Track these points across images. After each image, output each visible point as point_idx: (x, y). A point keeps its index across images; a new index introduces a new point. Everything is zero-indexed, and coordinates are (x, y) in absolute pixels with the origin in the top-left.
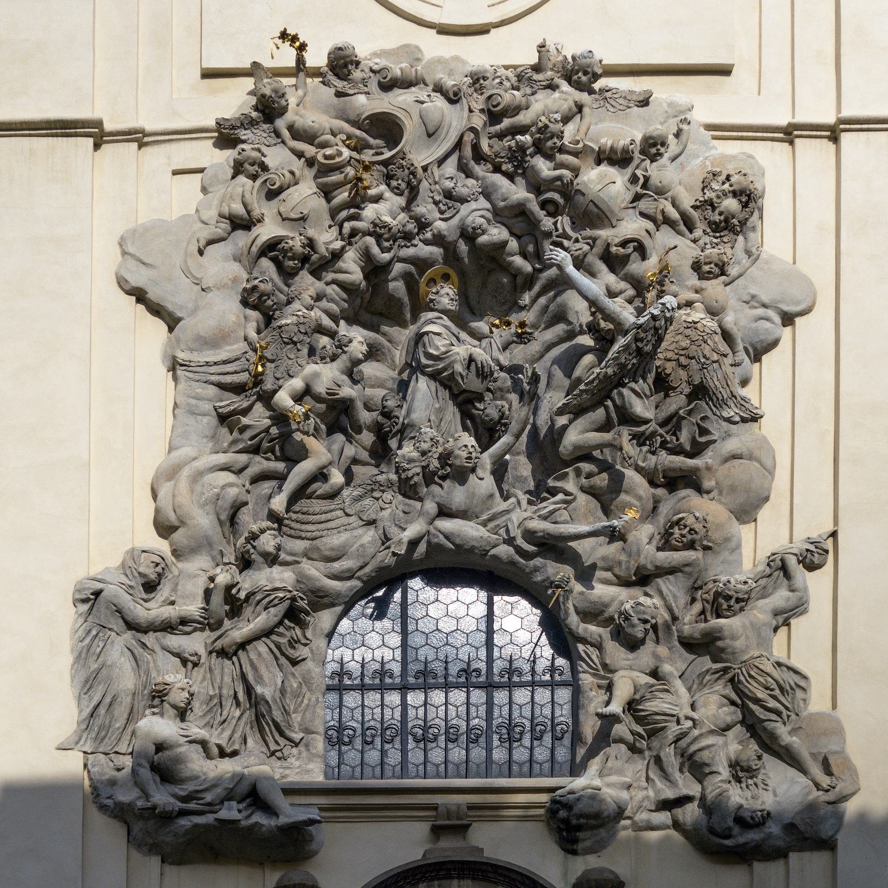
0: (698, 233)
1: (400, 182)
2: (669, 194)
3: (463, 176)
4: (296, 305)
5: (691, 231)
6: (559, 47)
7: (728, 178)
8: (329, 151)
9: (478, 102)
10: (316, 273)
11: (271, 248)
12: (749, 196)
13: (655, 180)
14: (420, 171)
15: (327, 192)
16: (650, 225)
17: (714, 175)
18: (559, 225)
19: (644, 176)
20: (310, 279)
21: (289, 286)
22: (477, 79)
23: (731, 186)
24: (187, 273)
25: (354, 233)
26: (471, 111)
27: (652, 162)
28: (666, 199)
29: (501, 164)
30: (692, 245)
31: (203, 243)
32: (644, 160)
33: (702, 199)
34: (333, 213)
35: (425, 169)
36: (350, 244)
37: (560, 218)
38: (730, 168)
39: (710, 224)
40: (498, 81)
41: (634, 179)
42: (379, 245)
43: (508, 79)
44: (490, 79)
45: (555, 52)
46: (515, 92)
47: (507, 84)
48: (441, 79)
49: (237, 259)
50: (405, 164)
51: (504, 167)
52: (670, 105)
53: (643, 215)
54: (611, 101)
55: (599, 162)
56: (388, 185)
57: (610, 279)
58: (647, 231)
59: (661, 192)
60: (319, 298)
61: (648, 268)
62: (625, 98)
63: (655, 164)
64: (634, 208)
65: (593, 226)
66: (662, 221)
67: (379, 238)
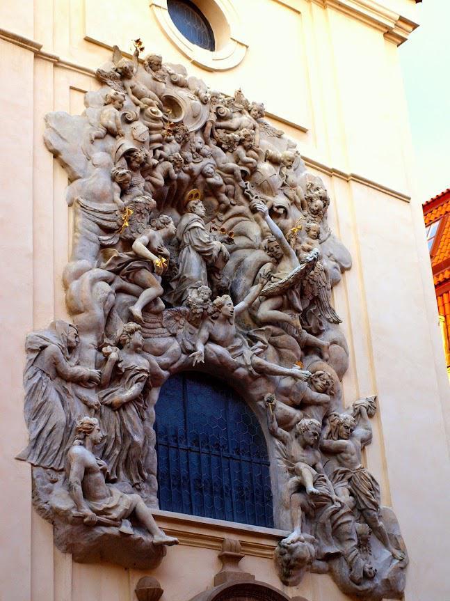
16: (289, 202)
26: (210, 111)
29: (222, 143)
51: (223, 146)
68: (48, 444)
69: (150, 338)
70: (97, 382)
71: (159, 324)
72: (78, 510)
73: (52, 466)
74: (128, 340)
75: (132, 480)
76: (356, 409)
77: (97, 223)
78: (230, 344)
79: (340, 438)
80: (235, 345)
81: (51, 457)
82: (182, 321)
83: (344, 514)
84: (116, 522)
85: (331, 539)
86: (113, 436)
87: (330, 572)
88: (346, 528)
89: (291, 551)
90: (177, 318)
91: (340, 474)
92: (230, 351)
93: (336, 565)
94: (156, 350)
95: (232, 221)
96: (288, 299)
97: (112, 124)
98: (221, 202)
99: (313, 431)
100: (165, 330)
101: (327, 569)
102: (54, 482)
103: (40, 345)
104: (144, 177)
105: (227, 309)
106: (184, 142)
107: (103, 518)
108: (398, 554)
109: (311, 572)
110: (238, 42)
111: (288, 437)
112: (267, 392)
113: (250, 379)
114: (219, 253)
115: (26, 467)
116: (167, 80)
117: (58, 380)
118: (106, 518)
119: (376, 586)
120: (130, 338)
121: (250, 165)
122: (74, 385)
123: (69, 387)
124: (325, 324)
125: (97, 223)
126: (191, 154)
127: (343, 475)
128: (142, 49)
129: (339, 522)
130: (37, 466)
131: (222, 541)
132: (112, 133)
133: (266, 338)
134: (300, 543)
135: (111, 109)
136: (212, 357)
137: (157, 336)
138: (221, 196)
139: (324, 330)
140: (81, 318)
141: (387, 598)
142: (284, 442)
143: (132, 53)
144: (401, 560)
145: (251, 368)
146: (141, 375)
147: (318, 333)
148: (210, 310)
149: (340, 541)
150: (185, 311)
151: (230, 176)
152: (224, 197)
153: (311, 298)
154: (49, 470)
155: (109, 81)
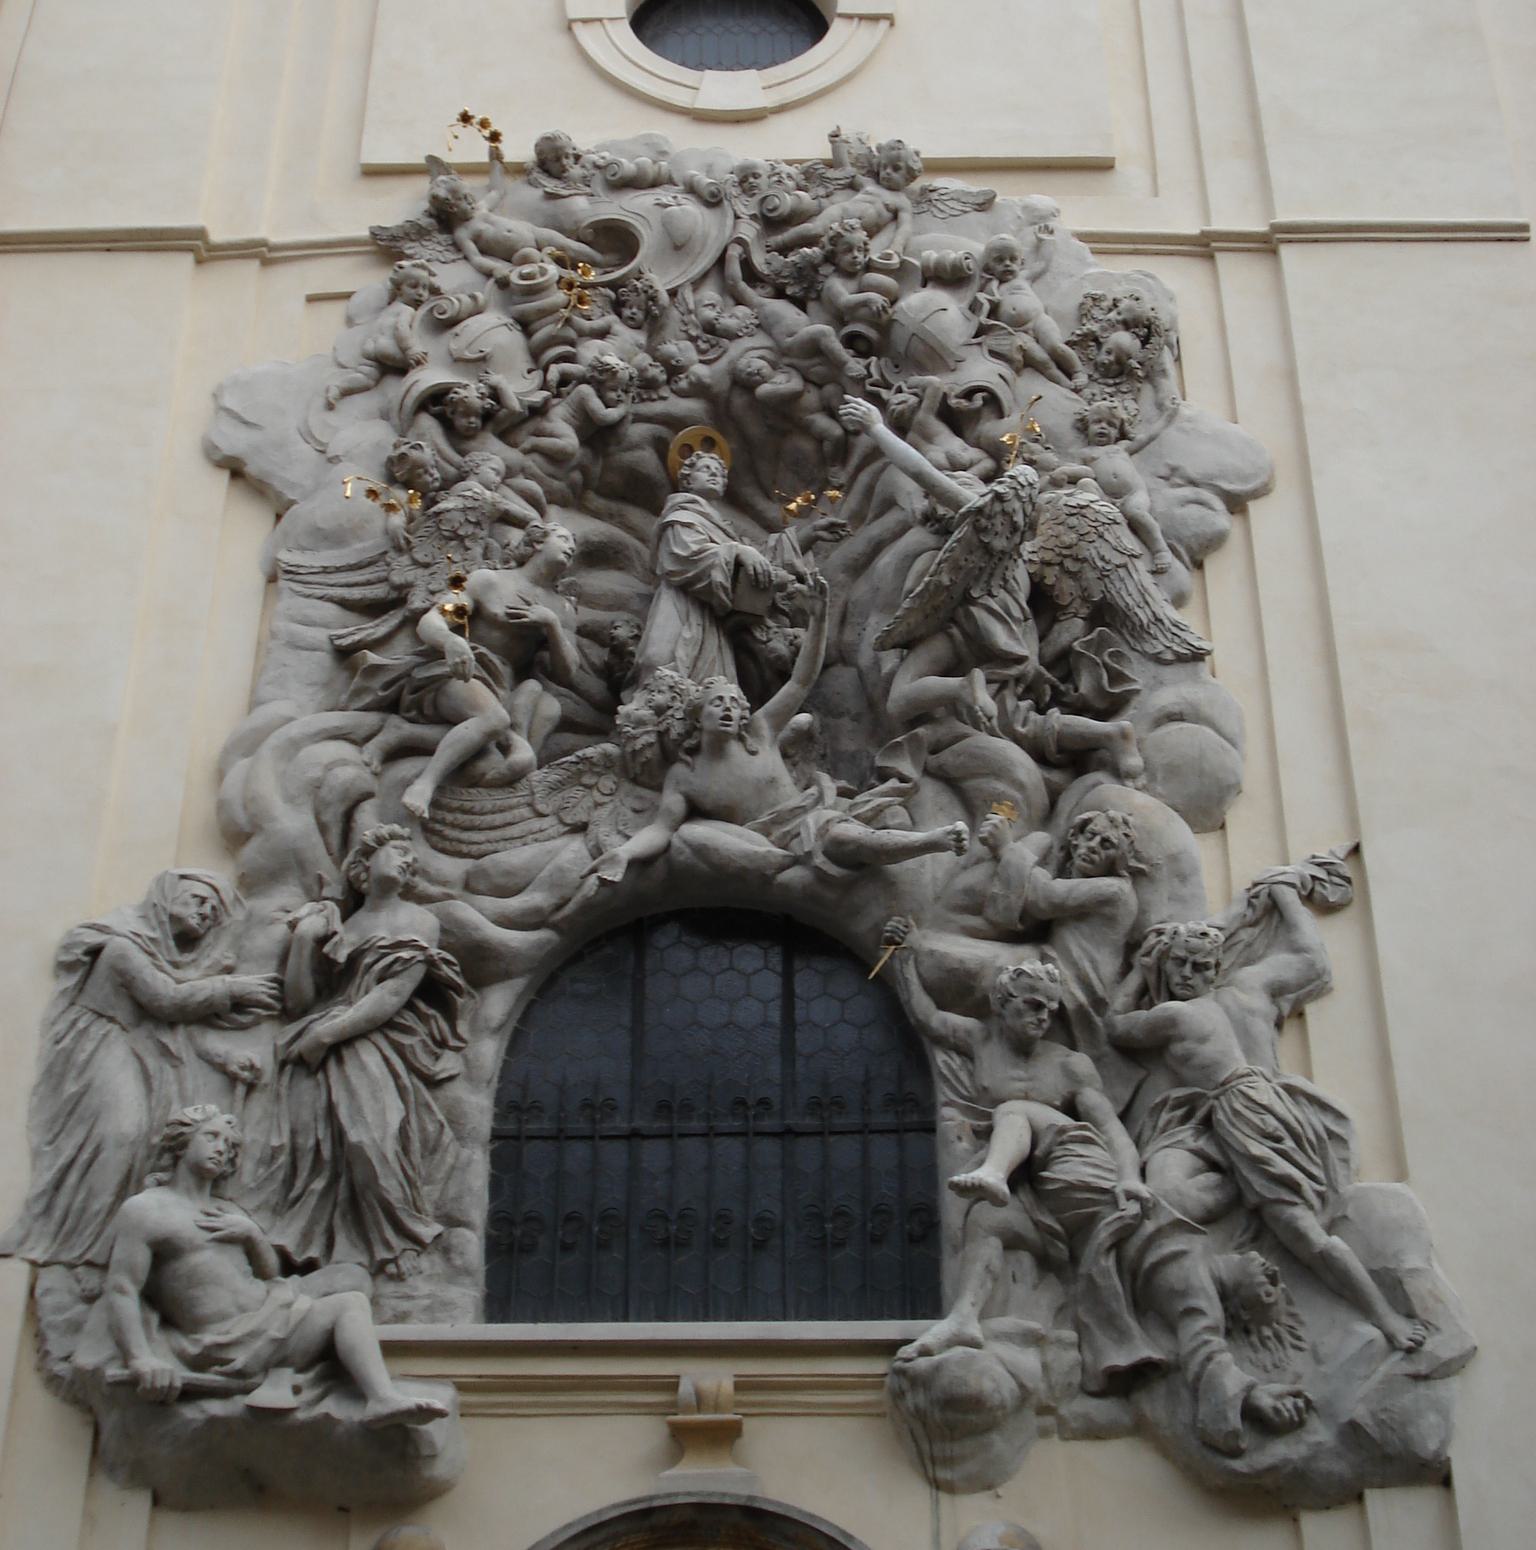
0: (1082, 379)
1: (635, 310)
2: (1030, 325)
3: (731, 302)
4: (473, 486)
5: (1070, 375)
6: (864, 138)
7: (1115, 303)
8: (526, 269)
9: (746, 207)
10: (505, 435)
11: (436, 401)
12: (1148, 327)
13: (1007, 308)
14: (664, 298)
15: (525, 325)
17: (1094, 299)
18: (873, 369)
19: (989, 301)
20: (495, 444)
21: (463, 453)
22: (746, 178)
23: (1119, 314)
24: (308, 436)
25: (565, 380)
26: (737, 217)
27: (1002, 282)
28: (1026, 332)
30: (1075, 396)
31: (334, 392)
32: (991, 280)
33: (1078, 332)
34: (535, 354)
35: (673, 293)
36: (558, 395)
37: (874, 359)
38: (1118, 291)
39: (1097, 366)
40: (775, 178)
41: (974, 307)
42: (601, 397)
43: (790, 176)
44: (764, 177)
45: (858, 143)
46: (801, 193)
47: (791, 184)
48: (693, 176)
49: (385, 416)
50: (639, 285)
51: (789, 291)
52: (1025, 208)
53: (994, 354)
54: (939, 205)
55: (924, 285)
56: (620, 315)
57: (956, 445)
58: (1001, 376)
59: (1019, 322)
60: (509, 473)
61: (1004, 431)
62: (958, 200)
63: (1005, 286)
64: (979, 344)
65: (923, 370)
66: (1029, 363)
67: (600, 388)
68: (81, 1197)
70: (267, 1007)
71: (525, 812)
72: (126, 1366)
73: (88, 1256)
74: (363, 876)
75: (371, 1253)
76: (1256, 896)
77: (321, 598)
78: (760, 811)
79: (1173, 997)
80: (778, 808)
81: (88, 1232)
82: (607, 783)
83: (1159, 1233)
84: (244, 1380)
85: (1130, 1321)
86: (311, 1142)
87: (1140, 1429)
88: (1173, 1275)
89: (918, 1381)
90: (587, 780)
91: (1174, 1108)
92: (767, 834)
93: (1154, 1404)
94: (501, 881)
95: (864, 478)
96: (964, 633)
97: (386, 344)
98: (820, 439)
99: (1028, 996)
100: (545, 823)
101: (1126, 1419)
102: (90, 1299)
103: (85, 948)
104: (514, 445)
105: (711, 715)
106: (651, 321)
107: (210, 1377)
108: (1403, 1330)
109: (1064, 1439)
110: (862, 17)
111: (969, 1033)
112: (889, 918)
113: (830, 895)
114: (735, 578)
115: (15, 1274)
116: (597, 186)
117: (148, 1027)
119: (1318, 1448)
120: (367, 869)
121: (863, 311)
122: (195, 1030)
123: (176, 1041)
124: (1139, 673)
125: (331, 600)
126: (689, 343)
127: (1179, 1112)
128: (495, 137)
129: (1151, 1258)
130: (45, 1265)
131: (671, 1385)
132: (392, 366)
133: (915, 761)
134: (959, 1350)
135: (404, 313)
136: (682, 858)
137: (518, 843)
138: (813, 421)
139: (1137, 692)
140: (251, 850)
141: (1382, 1486)
142: (966, 1053)
143: (485, 159)
144: (1409, 1351)
145: (820, 860)
146: (390, 958)
147: (1111, 707)
148: (677, 729)
149: (1171, 1327)
150: (606, 756)
151: (816, 360)
152: (822, 422)
153: (1084, 612)
154: (80, 1270)
155: (409, 248)
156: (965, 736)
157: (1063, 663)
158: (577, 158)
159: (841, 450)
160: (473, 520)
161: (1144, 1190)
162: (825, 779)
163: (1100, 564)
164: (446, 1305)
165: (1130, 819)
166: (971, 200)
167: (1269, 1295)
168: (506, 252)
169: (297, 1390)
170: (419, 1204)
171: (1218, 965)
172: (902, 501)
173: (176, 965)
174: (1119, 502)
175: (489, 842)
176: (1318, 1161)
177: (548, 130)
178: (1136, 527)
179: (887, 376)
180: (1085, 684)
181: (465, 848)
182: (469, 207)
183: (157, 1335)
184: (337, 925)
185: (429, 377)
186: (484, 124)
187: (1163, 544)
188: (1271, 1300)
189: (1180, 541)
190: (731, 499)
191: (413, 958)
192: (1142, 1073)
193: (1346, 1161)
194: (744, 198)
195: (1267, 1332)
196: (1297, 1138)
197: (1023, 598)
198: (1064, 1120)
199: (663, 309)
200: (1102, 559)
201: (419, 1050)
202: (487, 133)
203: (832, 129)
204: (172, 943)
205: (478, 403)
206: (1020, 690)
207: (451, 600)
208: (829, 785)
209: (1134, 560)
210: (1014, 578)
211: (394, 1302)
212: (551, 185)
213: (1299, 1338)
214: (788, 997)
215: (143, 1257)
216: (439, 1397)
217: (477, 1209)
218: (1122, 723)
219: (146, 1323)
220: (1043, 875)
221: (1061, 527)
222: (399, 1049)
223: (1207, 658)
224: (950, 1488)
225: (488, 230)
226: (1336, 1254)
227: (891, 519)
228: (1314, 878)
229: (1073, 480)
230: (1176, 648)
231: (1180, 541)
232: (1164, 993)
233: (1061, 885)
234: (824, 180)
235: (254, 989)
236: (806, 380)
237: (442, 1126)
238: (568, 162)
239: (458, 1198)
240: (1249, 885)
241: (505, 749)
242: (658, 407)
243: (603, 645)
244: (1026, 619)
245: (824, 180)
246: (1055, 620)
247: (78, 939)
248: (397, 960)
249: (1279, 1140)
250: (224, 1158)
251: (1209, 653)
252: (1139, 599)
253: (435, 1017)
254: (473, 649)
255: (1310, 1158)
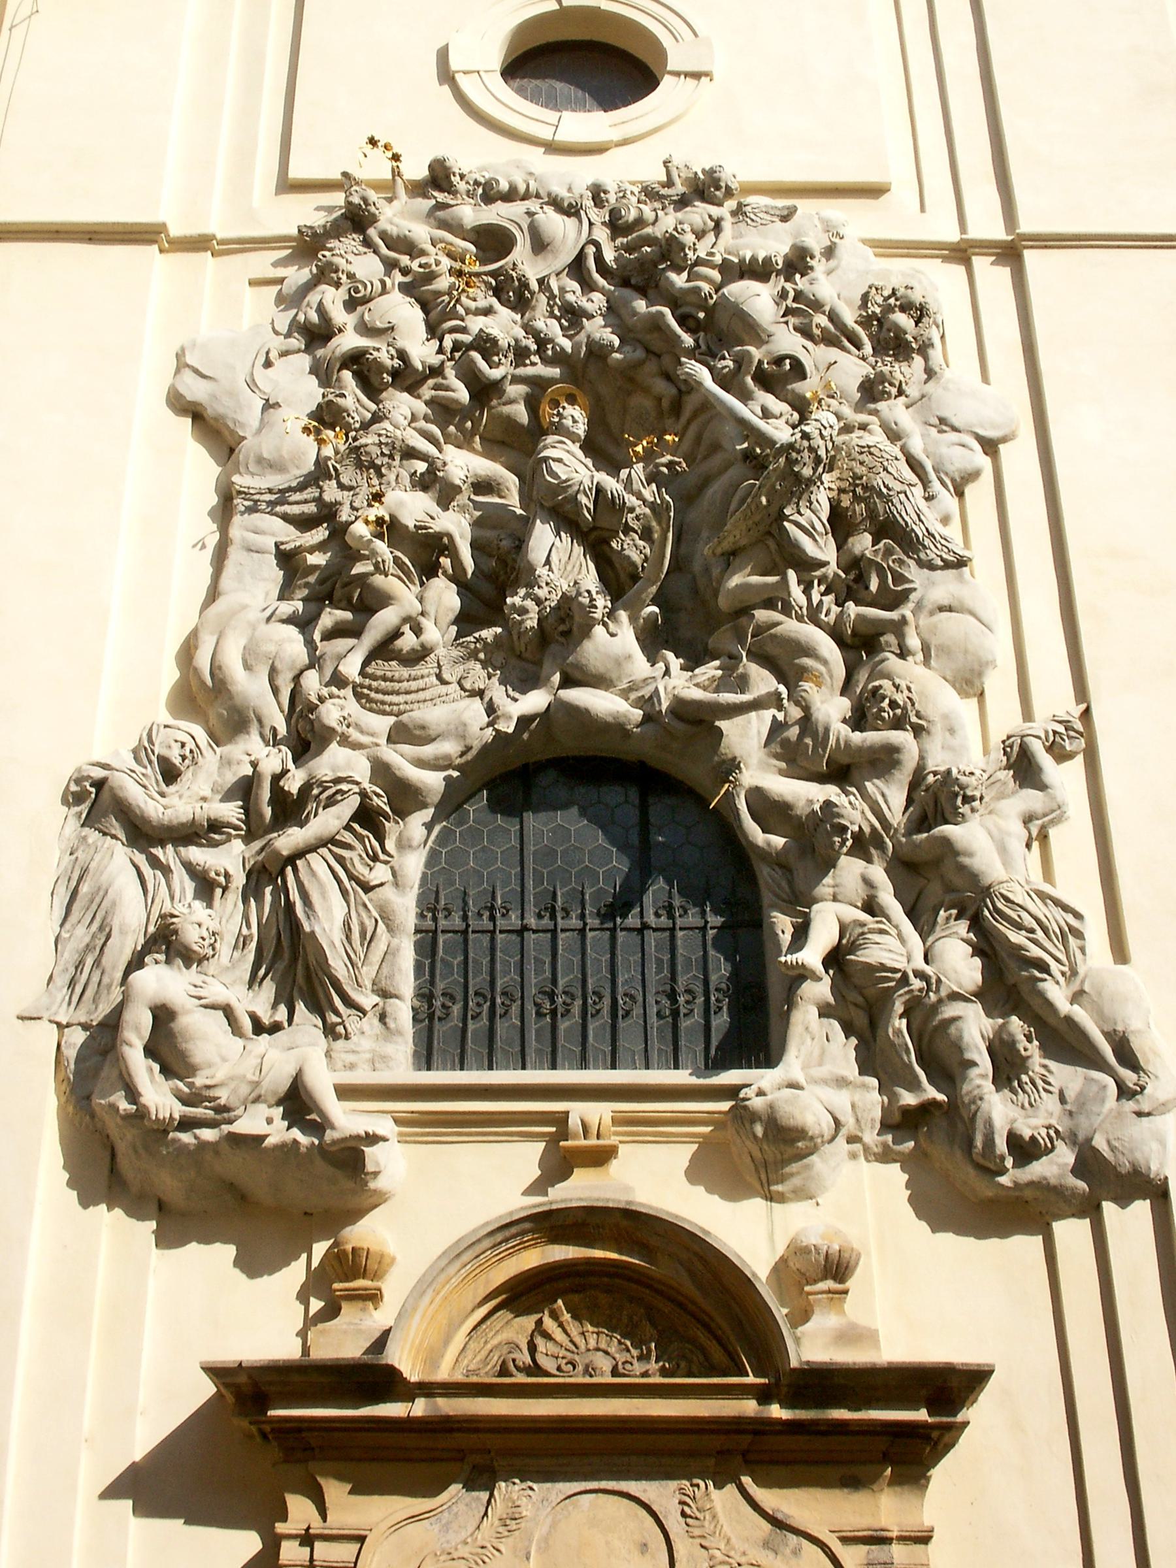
4: (386, 424)
9: (598, 216)
11: (356, 361)
14: (534, 286)
19: (794, 289)
23: (897, 300)
26: (591, 224)
35: (541, 282)
37: (702, 334)
59: (817, 305)
69: (412, 710)
70: (236, 828)
92: (627, 699)
104: (419, 397)
118: (206, 1108)
123: (166, 854)
139: (915, 589)
143: (388, 176)
147: (894, 600)
151: (656, 335)
156: (778, 624)
157: (856, 567)
158: (462, 177)
159: (676, 408)
160: (387, 452)
161: (928, 970)
162: (670, 655)
163: (884, 490)
164: (385, 1058)
165: (912, 686)
166: (778, 213)
167: (1026, 1050)
168: (408, 247)
169: (270, 1121)
170: (359, 980)
171: (982, 798)
172: (726, 444)
173: (163, 795)
174: (899, 444)
175: (406, 703)
176: (1062, 948)
177: (439, 154)
178: (914, 464)
179: (713, 347)
180: (874, 585)
181: (387, 708)
182: (377, 212)
183: (160, 1078)
184: (291, 765)
185: (349, 341)
186: (387, 147)
187: (932, 476)
188: (1028, 1053)
189: (947, 474)
190: (589, 446)
191: (350, 790)
192: (923, 881)
193: (1082, 950)
194: (596, 210)
195: (1025, 1078)
196: (1045, 931)
197: (825, 514)
198: (864, 917)
199: (532, 293)
200: (886, 487)
201: (357, 861)
202: (390, 154)
203: (665, 157)
204: (160, 778)
205: (389, 363)
206: (823, 588)
207: (373, 513)
208: (675, 663)
209: (912, 488)
210: (817, 501)
211: (343, 1056)
212: (441, 197)
213: (1049, 1084)
214: (645, 826)
215: (147, 1020)
216: (384, 1126)
217: (406, 983)
218: (906, 610)
219: (151, 1070)
220: (845, 730)
221: (853, 463)
222: (340, 860)
223: (969, 564)
224: (780, 1198)
225: (393, 230)
226: (1076, 1019)
227: (717, 460)
228: (1055, 732)
229: (863, 427)
230: (945, 556)
231: (947, 474)
232: (939, 817)
233: (857, 737)
234: (659, 197)
235: (226, 813)
236: (648, 351)
237: (376, 921)
238: (455, 180)
239: (391, 977)
240: (1005, 738)
241: (418, 630)
242: (529, 371)
243: (491, 556)
244: (827, 534)
245: (659, 197)
246: (849, 534)
247: (85, 774)
248: (338, 792)
249: (1032, 931)
250: (206, 943)
251: (970, 560)
252: (915, 518)
253: (368, 837)
254: (392, 553)
255: (1056, 946)
